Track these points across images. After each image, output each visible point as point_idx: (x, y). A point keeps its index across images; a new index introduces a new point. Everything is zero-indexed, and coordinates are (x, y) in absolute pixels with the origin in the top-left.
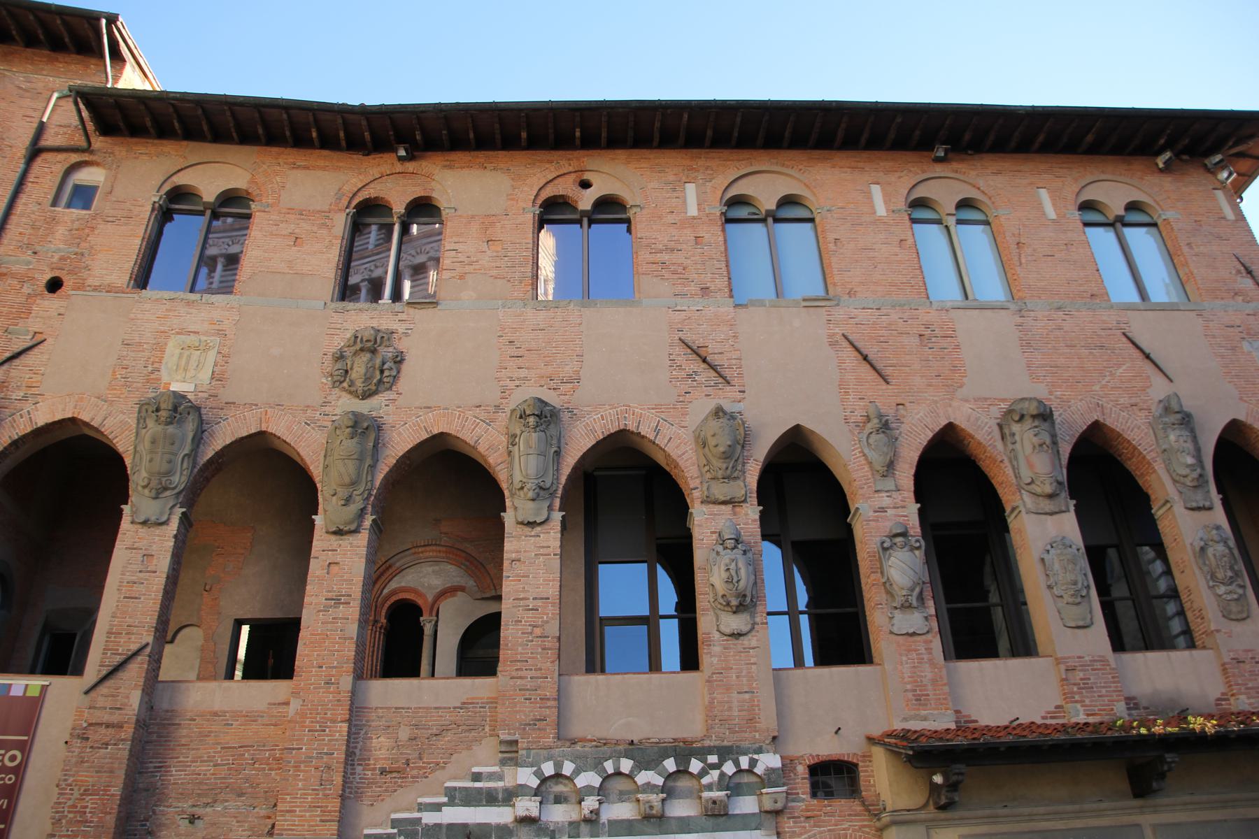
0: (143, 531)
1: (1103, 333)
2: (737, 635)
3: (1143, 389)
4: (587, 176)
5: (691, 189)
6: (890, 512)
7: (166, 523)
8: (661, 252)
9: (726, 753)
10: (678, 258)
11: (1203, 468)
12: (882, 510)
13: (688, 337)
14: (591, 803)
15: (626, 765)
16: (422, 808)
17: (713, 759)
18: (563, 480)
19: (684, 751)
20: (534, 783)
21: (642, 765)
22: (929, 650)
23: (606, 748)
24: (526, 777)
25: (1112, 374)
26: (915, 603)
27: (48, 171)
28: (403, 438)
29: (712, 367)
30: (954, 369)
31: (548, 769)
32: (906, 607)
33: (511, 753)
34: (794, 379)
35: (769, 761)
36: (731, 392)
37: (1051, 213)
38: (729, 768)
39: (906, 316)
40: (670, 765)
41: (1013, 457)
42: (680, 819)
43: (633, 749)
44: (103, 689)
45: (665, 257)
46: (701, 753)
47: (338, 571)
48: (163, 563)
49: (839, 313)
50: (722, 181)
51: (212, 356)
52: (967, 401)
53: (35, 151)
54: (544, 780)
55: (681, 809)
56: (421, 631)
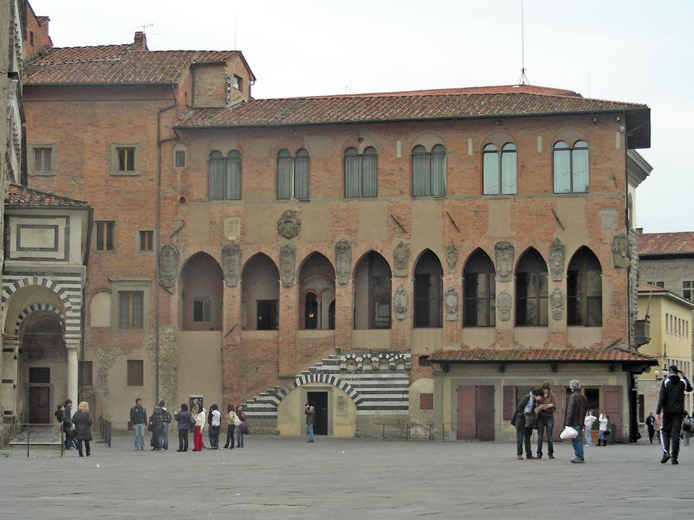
0: (230, 289)
1: (544, 208)
2: (401, 320)
3: (551, 233)
4: (361, 137)
5: (399, 143)
6: (453, 280)
7: (236, 286)
8: (386, 175)
9: (396, 353)
10: (393, 178)
11: (563, 265)
12: (450, 279)
13: (394, 213)
14: (359, 365)
15: (369, 356)
16: (316, 365)
17: (392, 355)
18: (353, 268)
19: (385, 352)
20: (345, 360)
21: (373, 355)
22: (457, 325)
23: (360, 352)
24: (343, 358)
25: (542, 227)
26: (454, 311)
27: (166, 148)
28: (302, 254)
29: (400, 226)
30: (484, 225)
31: (349, 356)
32: (452, 313)
33: (339, 351)
34: (428, 229)
35: (408, 356)
36: (407, 236)
37: (540, 149)
38: (396, 357)
39: (471, 203)
40: (381, 356)
41: (497, 261)
42: (384, 370)
43: (371, 351)
44: (229, 336)
45: (388, 178)
46: (389, 353)
47: (289, 302)
48: (238, 298)
49: (447, 202)
50: (410, 140)
51: (239, 226)
52: (485, 238)
53: (160, 143)
54: (348, 359)
55: (383, 367)
56: (317, 304)
